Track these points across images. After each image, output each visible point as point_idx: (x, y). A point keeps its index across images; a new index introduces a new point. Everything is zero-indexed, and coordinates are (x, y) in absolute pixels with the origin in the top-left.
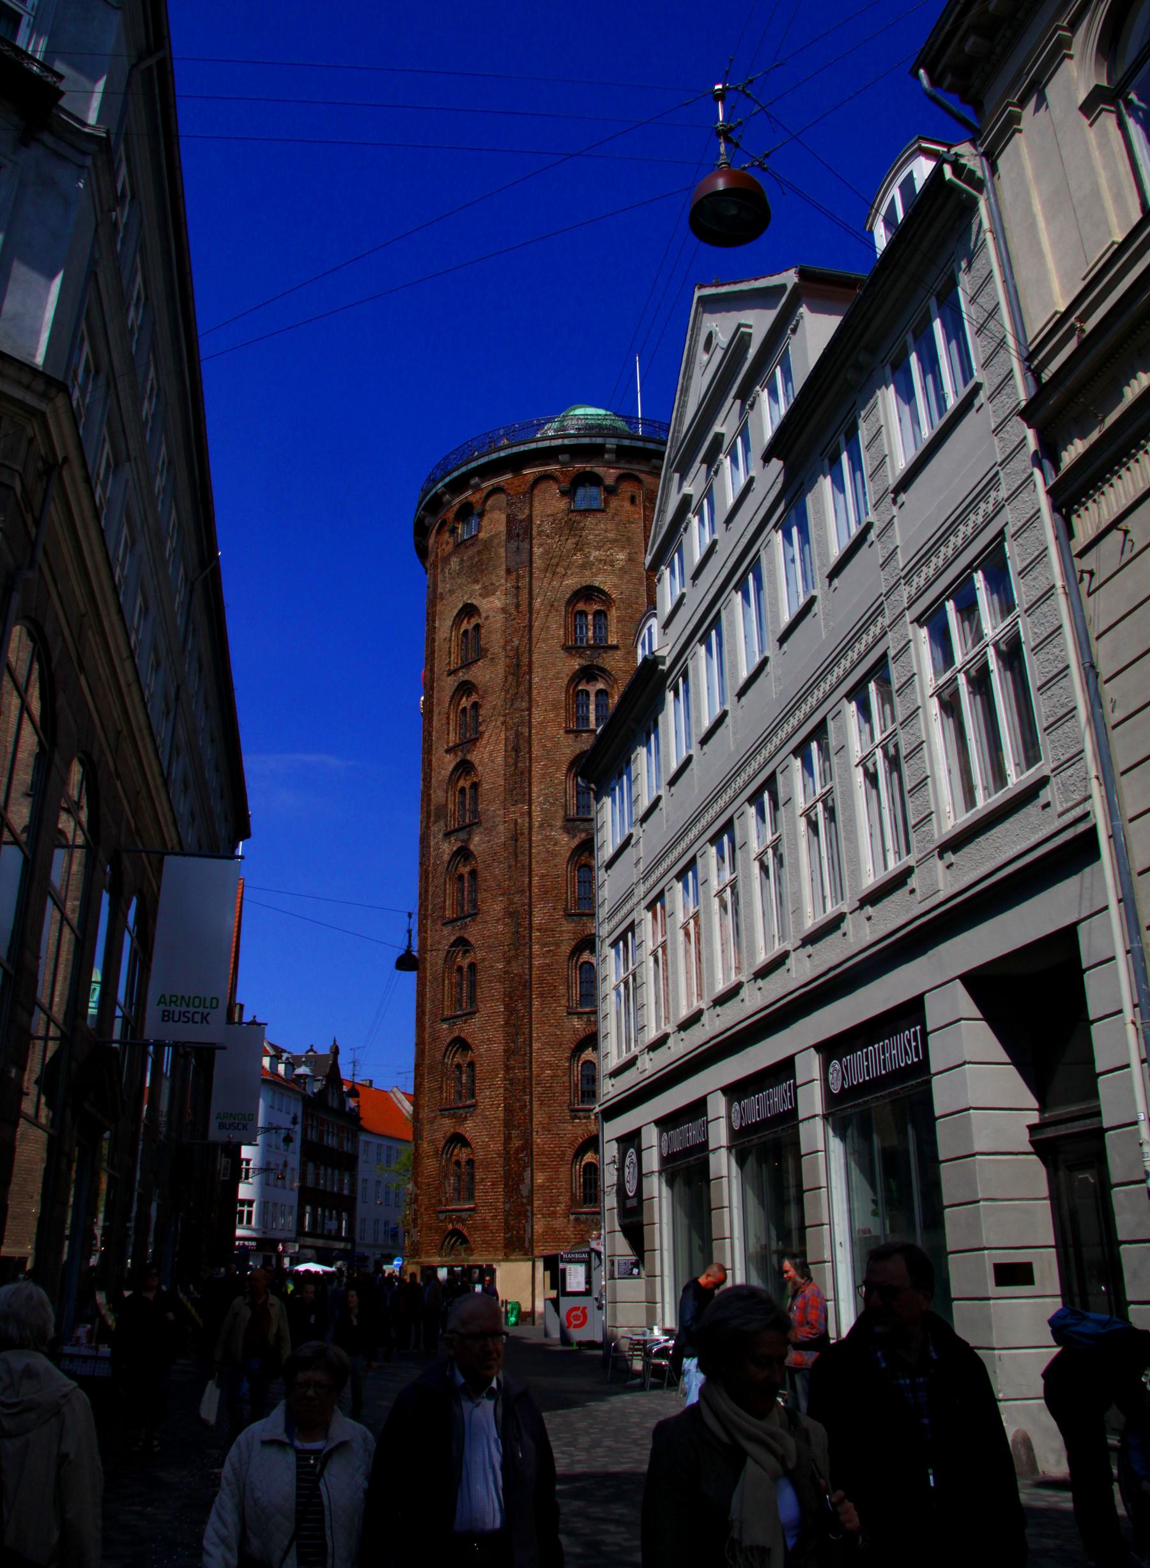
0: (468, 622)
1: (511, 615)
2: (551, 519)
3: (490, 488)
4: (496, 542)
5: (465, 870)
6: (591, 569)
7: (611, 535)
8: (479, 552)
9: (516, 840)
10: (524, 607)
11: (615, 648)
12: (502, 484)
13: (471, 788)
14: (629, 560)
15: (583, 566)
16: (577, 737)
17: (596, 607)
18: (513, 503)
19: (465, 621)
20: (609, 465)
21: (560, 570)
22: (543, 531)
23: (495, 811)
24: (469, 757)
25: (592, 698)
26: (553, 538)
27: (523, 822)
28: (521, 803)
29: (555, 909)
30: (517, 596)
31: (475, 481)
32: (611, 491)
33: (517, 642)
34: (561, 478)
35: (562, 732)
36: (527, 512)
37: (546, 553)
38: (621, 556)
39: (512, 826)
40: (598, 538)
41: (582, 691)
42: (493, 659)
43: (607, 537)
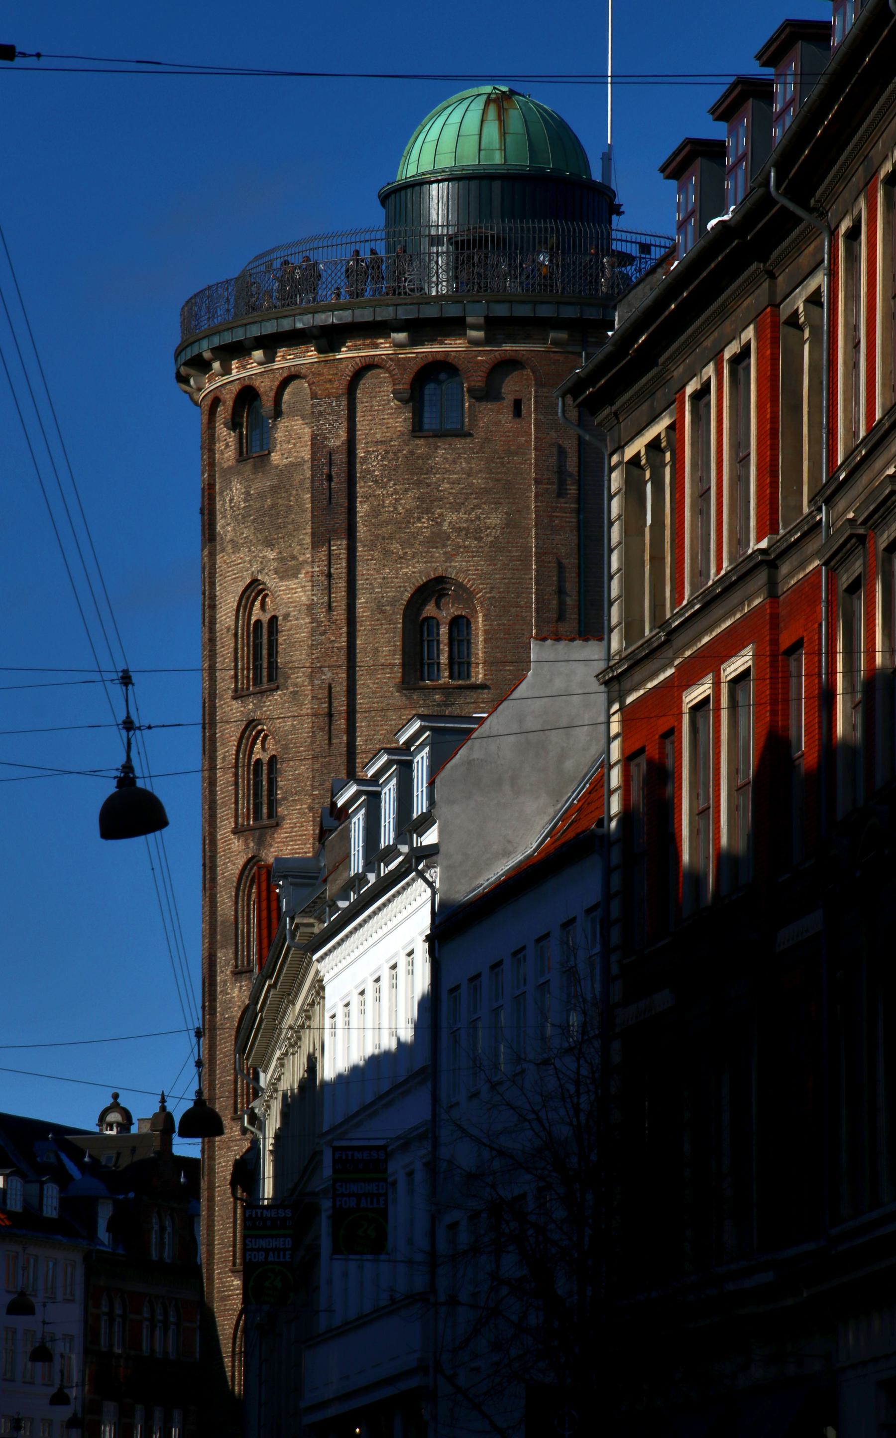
1: (319, 624)
2: (381, 449)
4: (297, 477)
6: (444, 546)
8: (274, 490)
10: (340, 614)
14: (507, 525)
18: (321, 414)
21: (395, 546)
26: (384, 487)
30: (329, 589)
33: (329, 674)
37: (375, 512)
40: (458, 487)
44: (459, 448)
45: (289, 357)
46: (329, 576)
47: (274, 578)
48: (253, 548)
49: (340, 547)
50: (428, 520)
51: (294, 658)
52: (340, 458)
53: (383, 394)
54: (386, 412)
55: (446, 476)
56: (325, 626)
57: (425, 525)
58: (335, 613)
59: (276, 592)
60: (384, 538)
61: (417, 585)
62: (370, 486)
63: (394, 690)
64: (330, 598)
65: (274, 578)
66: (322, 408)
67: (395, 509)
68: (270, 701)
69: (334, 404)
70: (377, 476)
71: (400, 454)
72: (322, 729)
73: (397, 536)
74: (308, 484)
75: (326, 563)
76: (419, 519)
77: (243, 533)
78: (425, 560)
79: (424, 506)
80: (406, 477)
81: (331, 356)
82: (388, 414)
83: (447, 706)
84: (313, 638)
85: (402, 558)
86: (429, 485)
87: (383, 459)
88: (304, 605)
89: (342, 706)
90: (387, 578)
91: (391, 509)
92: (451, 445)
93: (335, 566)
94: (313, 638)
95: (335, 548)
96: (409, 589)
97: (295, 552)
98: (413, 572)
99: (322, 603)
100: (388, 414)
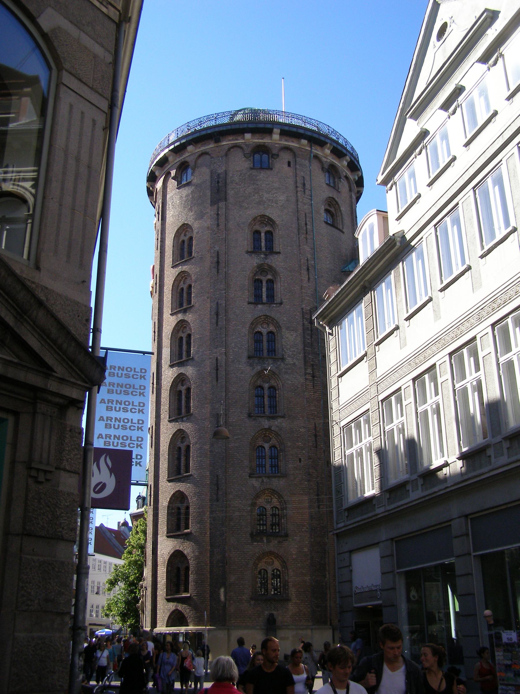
0: (185, 235)
3: (200, 153)
5: (183, 389)
7: (276, 185)
9: (217, 370)
11: (279, 253)
12: (208, 150)
13: (187, 337)
14: (287, 200)
15: (260, 203)
16: (255, 307)
17: (267, 228)
19: (183, 235)
21: (245, 205)
22: (234, 180)
23: (203, 352)
24: (186, 319)
25: (264, 284)
26: (240, 185)
27: (222, 359)
28: (221, 347)
29: (241, 413)
30: (218, 219)
31: (190, 148)
32: (275, 156)
34: (245, 148)
35: (246, 304)
36: (224, 168)
38: (282, 198)
39: (215, 361)
41: (258, 280)
46: (218, 214)
50: (258, 196)
60: (240, 202)
63: (245, 253)
67: (244, 192)
72: (215, 268)
76: (254, 195)
81: (220, 144)
83: (266, 259)
86: (257, 185)
87: (239, 176)
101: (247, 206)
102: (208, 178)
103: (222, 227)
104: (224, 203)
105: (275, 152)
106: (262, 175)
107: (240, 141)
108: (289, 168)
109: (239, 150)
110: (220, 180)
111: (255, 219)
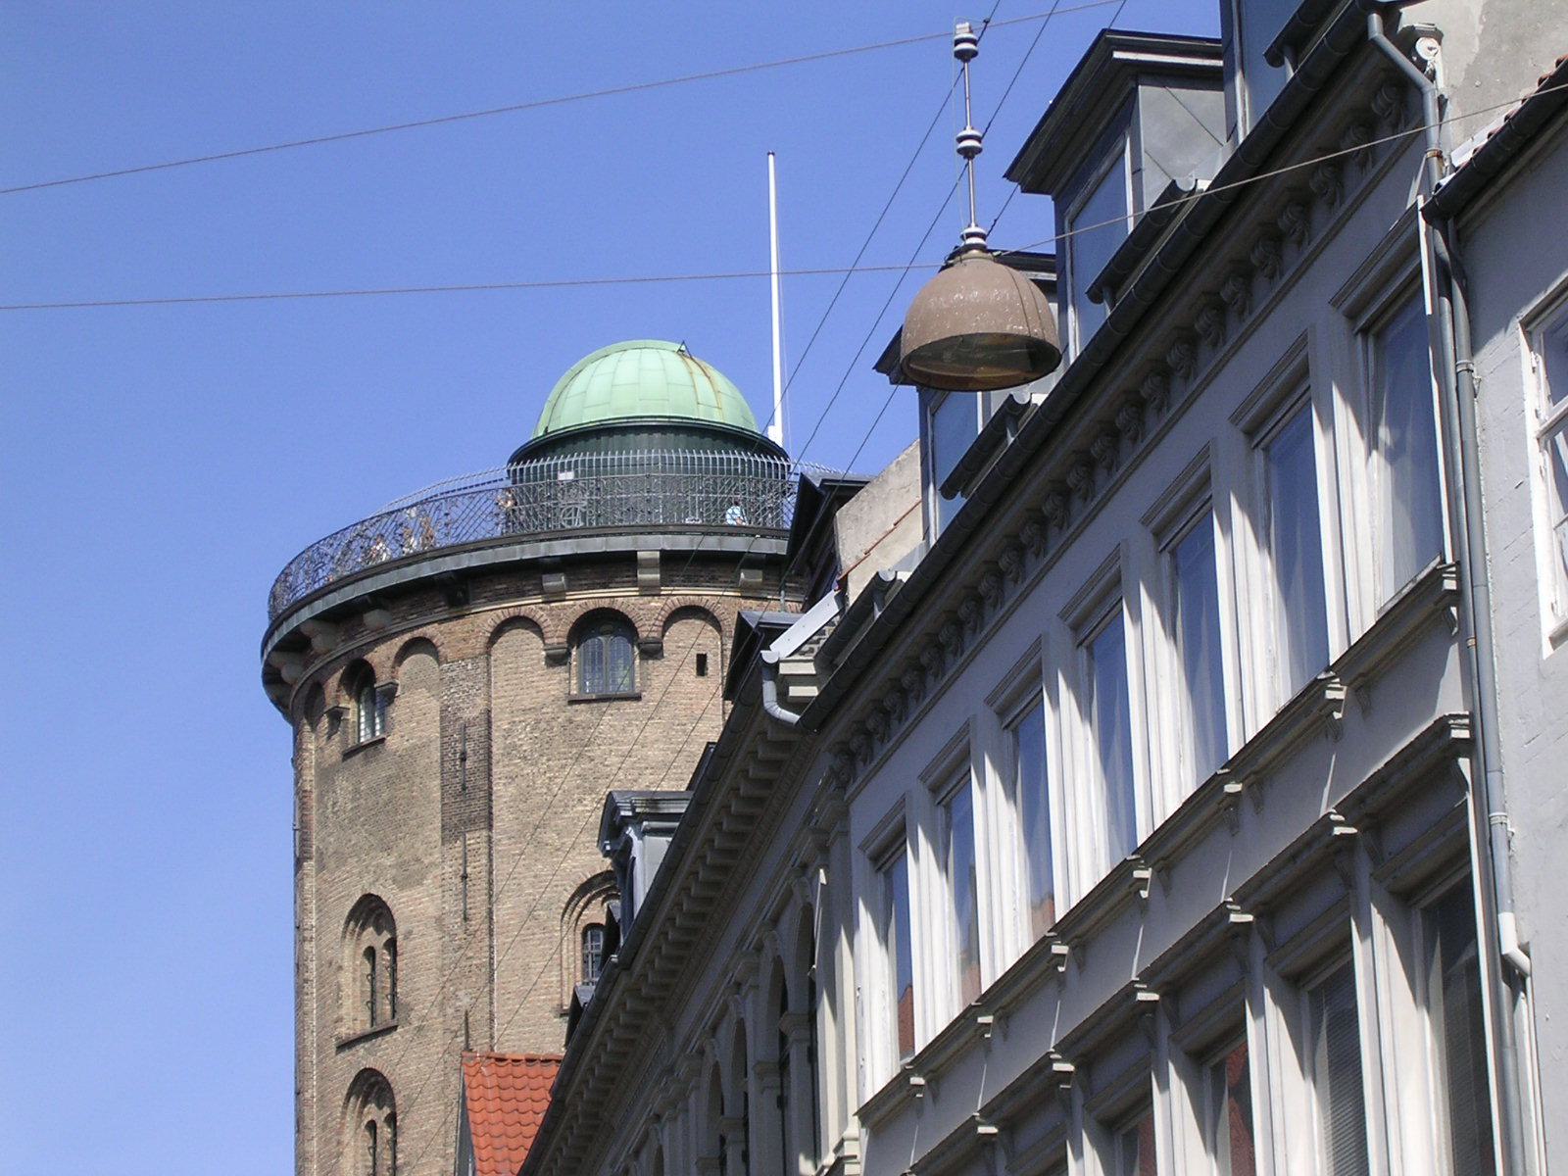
2: (531, 717)
4: (423, 762)
20: (649, 590)
21: (550, 836)
22: (515, 747)
36: (481, 702)
37: (524, 796)
42: (420, 1029)
43: (645, 758)
44: (628, 714)
45: (411, 617)
46: (465, 877)
47: (392, 889)
48: (363, 856)
49: (478, 840)
51: (418, 986)
52: (475, 732)
53: (531, 652)
54: (536, 674)
55: (613, 747)
56: (460, 939)
57: (588, 808)
58: (473, 922)
59: (395, 905)
61: (580, 882)
62: (516, 764)
64: (465, 904)
65: (392, 889)
66: (454, 673)
68: (387, 1042)
69: (469, 667)
70: (525, 751)
71: (554, 723)
73: (553, 823)
74: (436, 768)
75: (461, 861)
77: (350, 841)
78: (588, 851)
79: (586, 785)
80: (563, 750)
82: (538, 675)
84: (445, 956)
85: (558, 850)
87: (533, 729)
88: (431, 917)
89: (483, 1038)
90: (541, 876)
91: (545, 790)
92: (619, 709)
93: (473, 864)
94: (445, 956)
95: (472, 841)
96: (569, 888)
97: (419, 854)
98: (574, 867)
99: (456, 912)
100: (538, 675)
101: (557, 844)
102: (434, 732)
103: (478, 920)
104: (485, 833)
105: (647, 629)
106: (612, 718)
107: (531, 605)
108: (701, 679)
109: (529, 635)
110: (470, 747)
111: (584, 889)
